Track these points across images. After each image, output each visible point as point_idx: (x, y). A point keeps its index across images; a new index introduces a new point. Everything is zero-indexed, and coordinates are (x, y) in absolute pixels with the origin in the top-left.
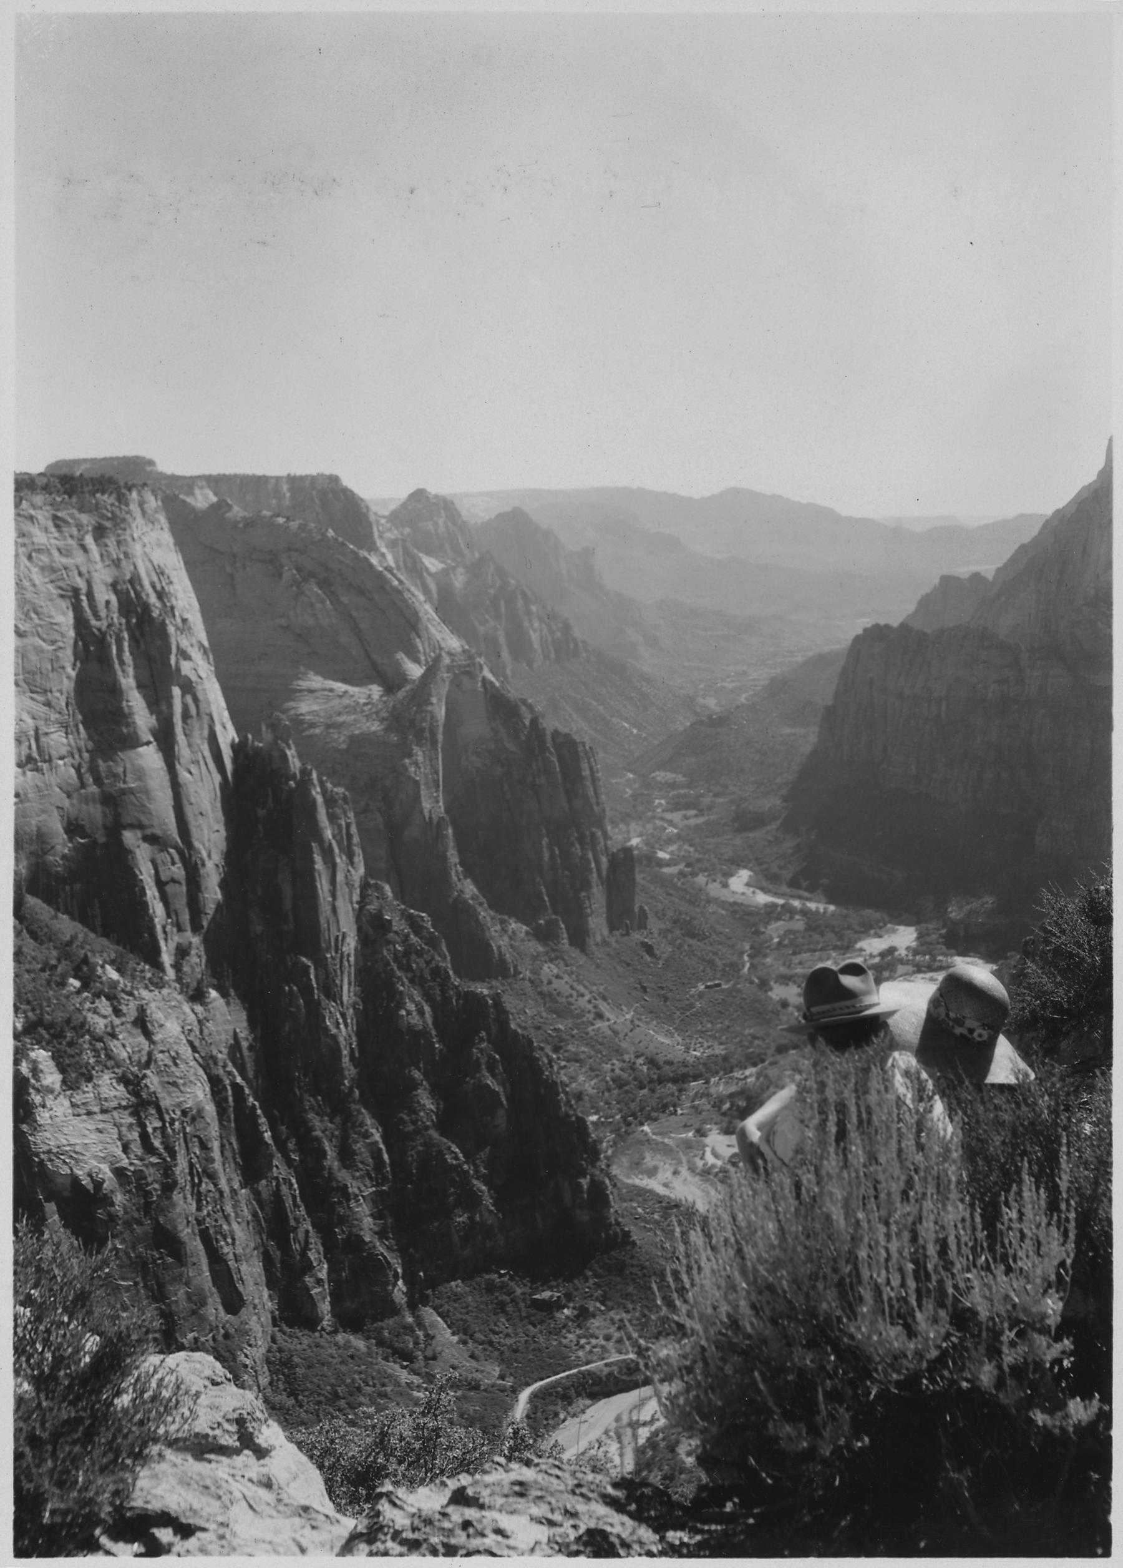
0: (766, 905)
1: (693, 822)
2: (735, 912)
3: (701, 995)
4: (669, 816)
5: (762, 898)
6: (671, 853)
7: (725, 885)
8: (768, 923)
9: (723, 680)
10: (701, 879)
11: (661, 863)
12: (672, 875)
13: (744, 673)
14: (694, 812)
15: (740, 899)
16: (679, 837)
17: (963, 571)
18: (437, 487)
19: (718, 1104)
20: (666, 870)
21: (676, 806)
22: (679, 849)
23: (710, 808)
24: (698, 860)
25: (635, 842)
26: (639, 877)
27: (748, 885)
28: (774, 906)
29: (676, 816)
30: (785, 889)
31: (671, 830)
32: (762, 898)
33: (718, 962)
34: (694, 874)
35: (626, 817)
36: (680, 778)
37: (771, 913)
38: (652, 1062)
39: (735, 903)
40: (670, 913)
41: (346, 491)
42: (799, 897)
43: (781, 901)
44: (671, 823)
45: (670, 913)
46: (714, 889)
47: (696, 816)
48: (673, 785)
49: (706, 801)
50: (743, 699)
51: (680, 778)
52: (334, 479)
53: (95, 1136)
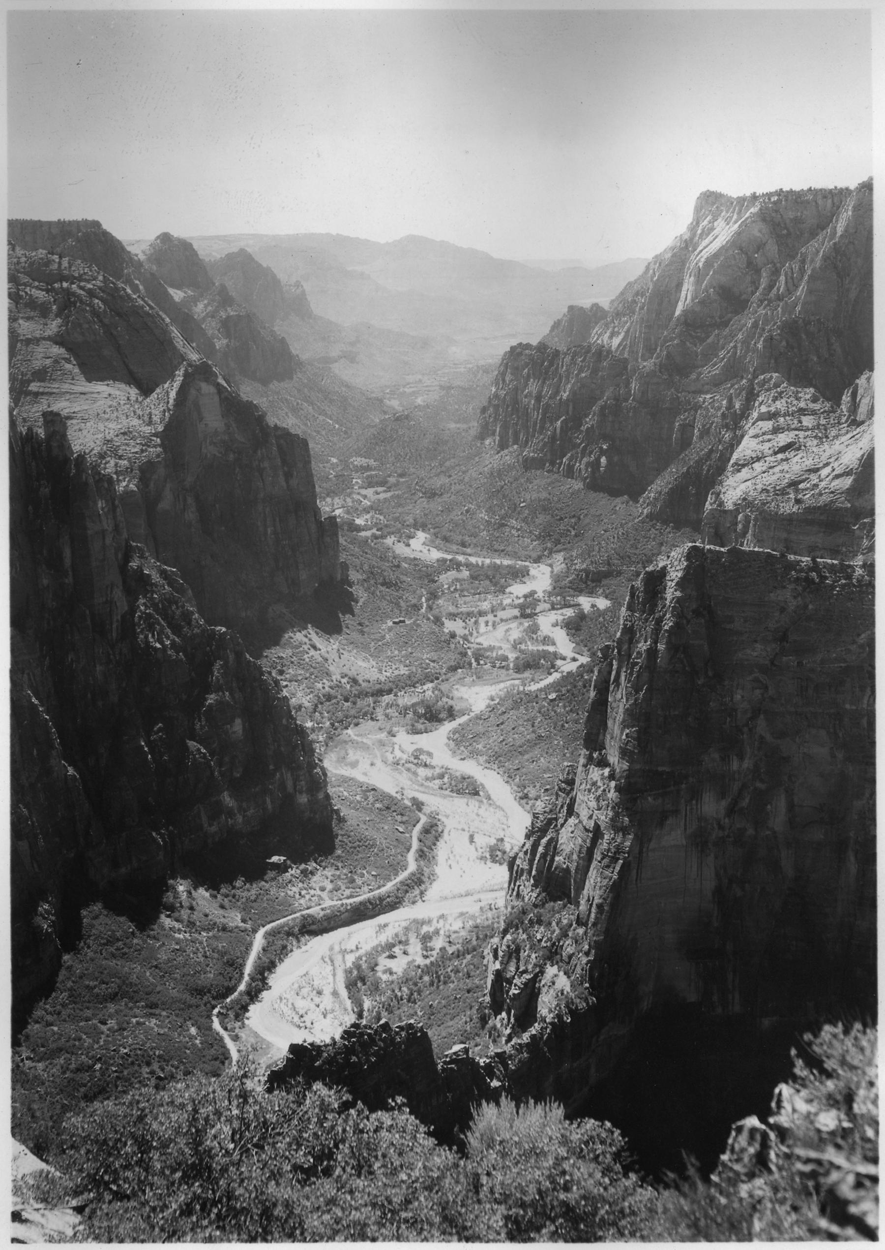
0: (438, 560)
1: (382, 496)
2: (416, 565)
3: (390, 629)
4: (363, 492)
5: (435, 555)
6: (367, 520)
7: (408, 545)
8: (439, 573)
9: (404, 386)
10: (389, 541)
11: (359, 529)
12: (367, 538)
13: (420, 381)
14: (380, 489)
15: (418, 555)
16: (371, 507)
17: (586, 303)
18: (178, 232)
19: (406, 708)
20: (363, 534)
21: (370, 485)
22: (372, 517)
23: (397, 485)
24: (386, 526)
25: (337, 512)
26: (341, 540)
27: (424, 544)
28: (444, 560)
29: (369, 492)
30: (455, 547)
31: (367, 503)
32: (435, 555)
33: (402, 604)
34: (383, 537)
35: (331, 493)
36: (372, 462)
37: (444, 566)
38: (354, 681)
39: (415, 559)
40: (366, 567)
41: (106, 234)
42: (464, 554)
43: (449, 557)
44: (365, 497)
45: (366, 567)
46: (400, 549)
47: (385, 491)
48: (368, 468)
49: (392, 480)
50: (419, 401)
51: (372, 462)
52: (96, 224)
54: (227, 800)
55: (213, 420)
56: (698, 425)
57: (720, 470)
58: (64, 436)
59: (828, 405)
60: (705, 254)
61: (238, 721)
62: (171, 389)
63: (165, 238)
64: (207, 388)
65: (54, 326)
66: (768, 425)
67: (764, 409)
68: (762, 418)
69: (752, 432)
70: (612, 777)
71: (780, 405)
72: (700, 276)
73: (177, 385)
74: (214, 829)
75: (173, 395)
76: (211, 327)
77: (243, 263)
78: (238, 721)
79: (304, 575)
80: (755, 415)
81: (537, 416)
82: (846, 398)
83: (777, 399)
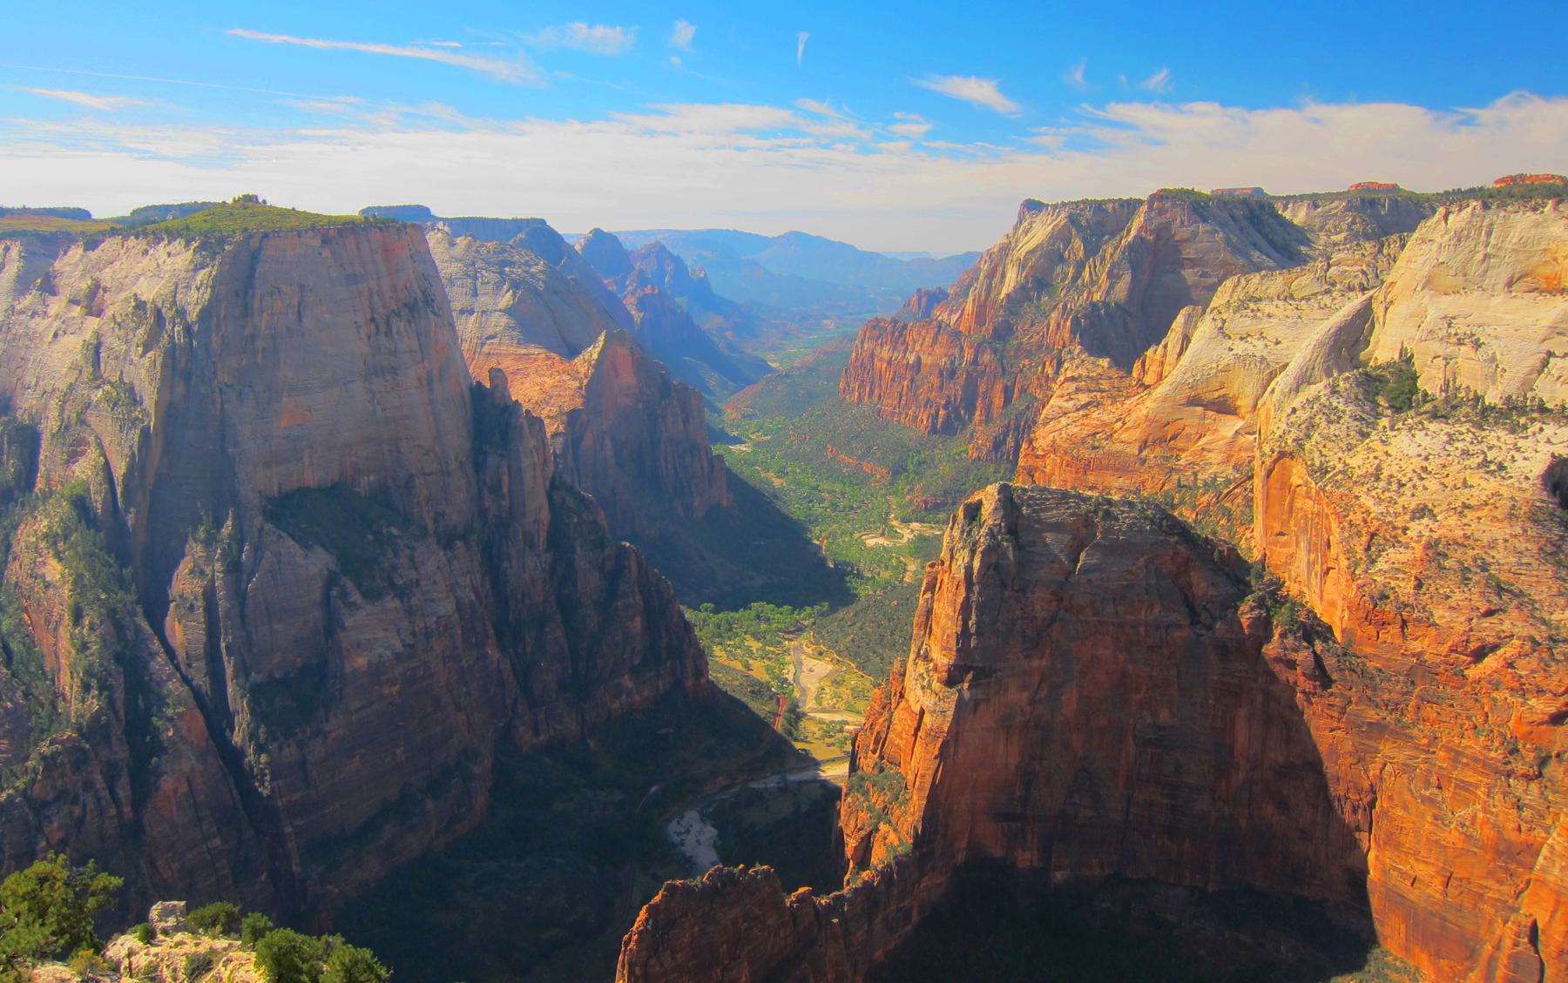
53: (381, 634)
54: (628, 682)
55: (627, 378)
56: (1018, 386)
57: (1031, 425)
58: (506, 389)
59: (1122, 373)
60: (1025, 249)
61: (638, 619)
62: (593, 353)
63: (597, 232)
64: (622, 351)
65: (506, 300)
66: (1072, 386)
67: (1069, 374)
68: (1067, 380)
69: (1059, 392)
70: (935, 669)
71: (1082, 371)
72: (1022, 265)
73: (597, 350)
74: (616, 705)
75: (595, 356)
76: (630, 304)
77: (659, 252)
78: (638, 619)
79: (696, 503)
80: (1062, 378)
81: (888, 376)
82: (1137, 365)
83: (1080, 364)
